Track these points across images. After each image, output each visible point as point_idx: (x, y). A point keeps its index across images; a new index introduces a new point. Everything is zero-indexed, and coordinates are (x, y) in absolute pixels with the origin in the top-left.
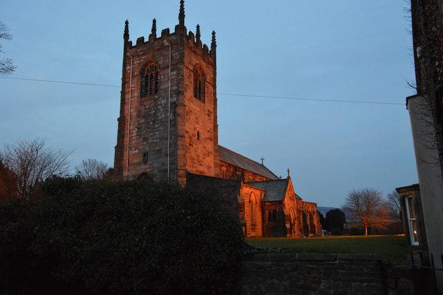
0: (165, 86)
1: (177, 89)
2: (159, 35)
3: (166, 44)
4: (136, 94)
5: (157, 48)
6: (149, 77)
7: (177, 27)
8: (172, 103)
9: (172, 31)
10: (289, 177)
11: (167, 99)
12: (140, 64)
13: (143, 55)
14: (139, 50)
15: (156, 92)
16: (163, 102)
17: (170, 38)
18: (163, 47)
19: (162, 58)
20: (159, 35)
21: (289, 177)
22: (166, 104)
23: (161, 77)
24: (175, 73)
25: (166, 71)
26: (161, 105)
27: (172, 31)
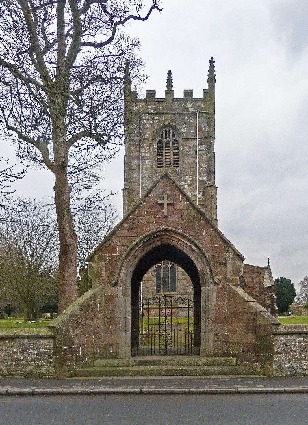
0: (191, 160)
1: (207, 168)
2: (179, 94)
3: (191, 110)
4: (148, 162)
5: (180, 111)
6: (164, 145)
7: (205, 92)
8: (201, 182)
9: (198, 94)
10: (269, 265)
11: (194, 176)
12: (152, 124)
13: (158, 114)
14: (150, 107)
15: (175, 163)
16: (189, 178)
17: (197, 104)
18: (186, 112)
19: (185, 125)
20: (179, 94)
21: (269, 265)
22: (194, 180)
23: (184, 147)
24: (204, 147)
25: (192, 143)
26: (186, 181)
27: (198, 94)
